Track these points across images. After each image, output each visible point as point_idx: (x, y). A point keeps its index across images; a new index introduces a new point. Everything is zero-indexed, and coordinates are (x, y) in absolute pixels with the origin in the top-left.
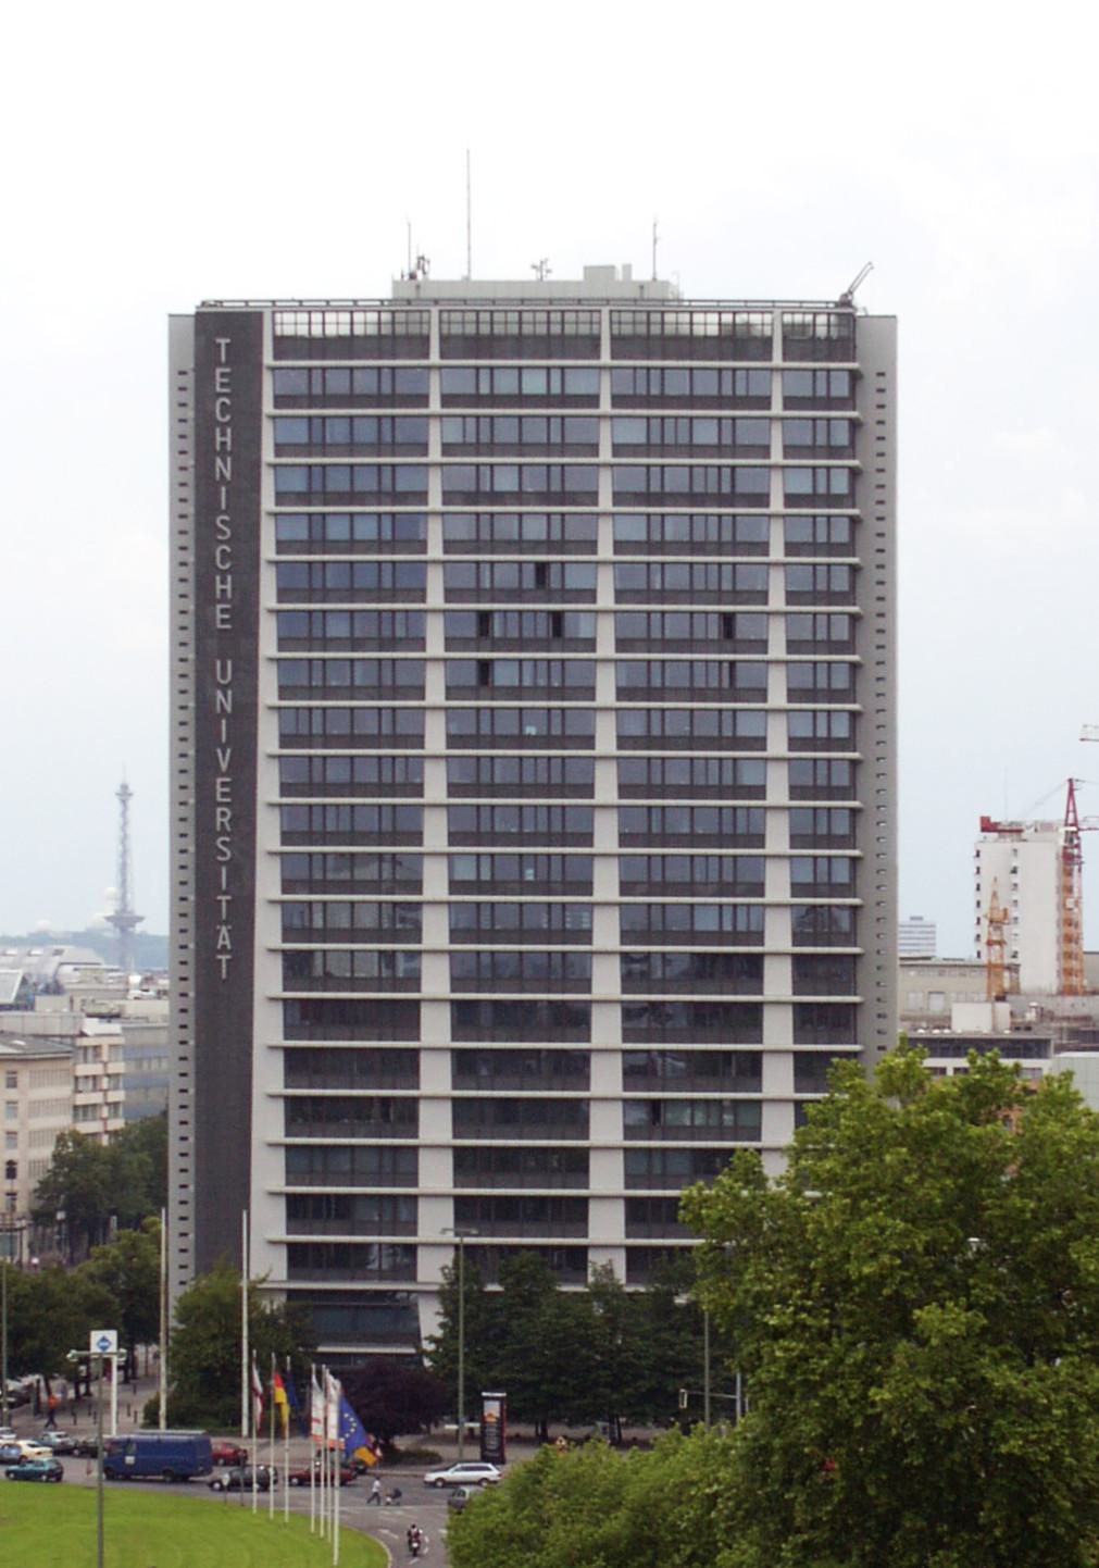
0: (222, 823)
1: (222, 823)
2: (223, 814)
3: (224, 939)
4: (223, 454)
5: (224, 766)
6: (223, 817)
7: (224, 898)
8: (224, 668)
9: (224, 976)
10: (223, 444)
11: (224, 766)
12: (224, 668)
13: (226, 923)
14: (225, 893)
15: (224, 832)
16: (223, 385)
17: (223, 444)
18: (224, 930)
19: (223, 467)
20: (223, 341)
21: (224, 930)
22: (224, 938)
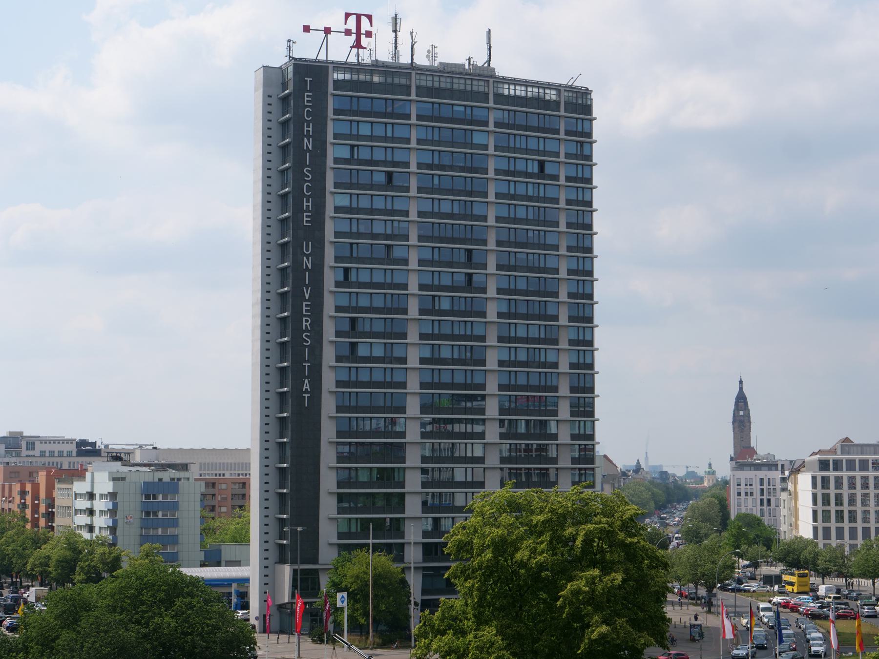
0: (306, 325)
1: (306, 325)
2: (308, 321)
3: (306, 386)
4: (308, 137)
5: (307, 297)
6: (306, 323)
7: (307, 365)
9: (306, 406)
11: (307, 297)
13: (307, 377)
15: (307, 330)
18: (306, 380)
20: (309, 79)
21: (306, 380)
22: (306, 385)
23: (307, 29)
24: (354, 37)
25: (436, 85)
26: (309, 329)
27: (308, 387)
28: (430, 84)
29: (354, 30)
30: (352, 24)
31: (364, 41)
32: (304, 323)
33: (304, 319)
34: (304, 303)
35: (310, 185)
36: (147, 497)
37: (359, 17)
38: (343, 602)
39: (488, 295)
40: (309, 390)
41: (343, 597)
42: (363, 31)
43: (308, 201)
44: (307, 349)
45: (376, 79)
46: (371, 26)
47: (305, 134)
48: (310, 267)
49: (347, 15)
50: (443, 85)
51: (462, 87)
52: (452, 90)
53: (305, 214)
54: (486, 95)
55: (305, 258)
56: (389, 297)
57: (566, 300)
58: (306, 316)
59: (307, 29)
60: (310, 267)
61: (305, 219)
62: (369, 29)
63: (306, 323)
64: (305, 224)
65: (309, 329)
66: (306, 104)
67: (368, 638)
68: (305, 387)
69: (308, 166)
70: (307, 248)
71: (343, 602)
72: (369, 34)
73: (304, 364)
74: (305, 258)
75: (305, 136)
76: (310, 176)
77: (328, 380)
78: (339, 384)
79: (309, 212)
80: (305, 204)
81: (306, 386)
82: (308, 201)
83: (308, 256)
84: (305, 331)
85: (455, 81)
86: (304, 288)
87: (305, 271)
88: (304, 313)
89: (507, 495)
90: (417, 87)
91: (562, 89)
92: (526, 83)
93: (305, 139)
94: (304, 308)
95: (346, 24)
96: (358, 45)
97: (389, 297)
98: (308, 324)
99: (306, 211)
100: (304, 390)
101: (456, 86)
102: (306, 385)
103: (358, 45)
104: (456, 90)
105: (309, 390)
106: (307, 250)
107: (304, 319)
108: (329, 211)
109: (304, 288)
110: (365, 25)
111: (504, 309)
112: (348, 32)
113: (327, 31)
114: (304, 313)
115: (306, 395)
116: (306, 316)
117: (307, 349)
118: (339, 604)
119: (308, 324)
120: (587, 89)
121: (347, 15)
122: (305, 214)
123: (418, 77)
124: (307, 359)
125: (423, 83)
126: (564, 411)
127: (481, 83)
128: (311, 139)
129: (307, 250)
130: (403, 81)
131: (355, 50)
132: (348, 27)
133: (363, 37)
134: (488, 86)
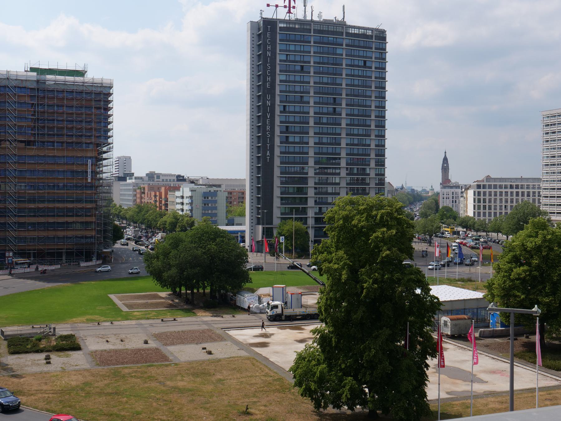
2: (268, 127)
4: (269, 51)
5: (268, 117)
6: (268, 128)
7: (268, 145)
10: (269, 49)
11: (268, 117)
15: (268, 131)
16: (269, 36)
17: (269, 49)
18: (268, 152)
20: (269, 27)
21: (268, 152)
22: (268, 154)
24: (288, 8)
25: (322, 29)
28: (319, 28)
29: (288, 6)
31: (292, 10)
36: (205, 198)
38: (282, 240)
39: (342, 116)
41: (283, 238)
42: (292, 6)
43: (269, 78)
45: (297, 26)
50: (324, 29)
51: (332, 30)
52: (328, 31)
54: (343, 33)
55: (268, 101)
56: (302, 117)
58: (268, 125)
59: (268, 5)
62: (294, 5)
63: (268, 128)
67: (292, 255)
69: (269, 63)
70: (269, 97)
71: (282, 240)
72: (294, 7)
74: (268, 101)
77: (277, 151)
78: (281, 153)
79: (269, 82)
82: (269, 78)
83: (269, 101)
85: (330, 27)
90: (314, 30)
91: (374, 30)
92: (359, 28)
93: (268, 52)
94: (267, 122)
96: (289, 12)
97: (302, 117)
99: (268, 82)
101: (330, 29)
102: (268, 154)
103: (289, 12)
104: (330, 31)
106: (269, 98)
108: (278, 82)
111: (349, 122)
112: (285, 7)
113: (277, 6)
115: (268, 157)
116: (268, 125)
118: (281, 241)
120: (384, 30)
123: (314, 25)
125: (316, 28)
126: (373, 164)
127: (340, 28)
129: (269, 98)
130: (308, 27)
131: (288, 14)
133: (291, 9)
134: (343, 29)
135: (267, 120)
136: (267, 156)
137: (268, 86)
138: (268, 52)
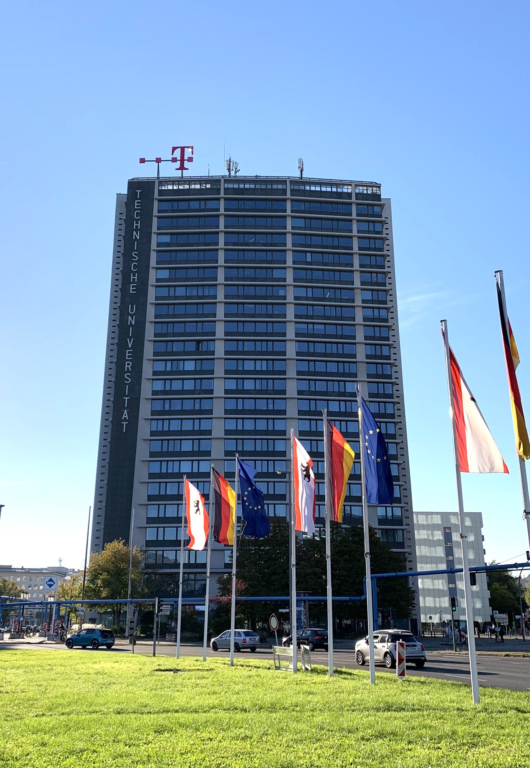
0: (128, 368)
1: (128, 368)
2: (129, 364)
3: (125, 415)
4: (137, 230)
5: (130, 346)
6: (128, 366)
7: (126, 398)
8: (132, 308)
10: (137, 227)
11: (130, 346)
12: (132, 308)
13: (126, 408)
14: (127, 396)
15: (128, 371)
16: (137, 206)
17: (137, 227)
19: (136, 235)
20: (139, 191)
22: (125, 415)
23: (142, 161)
24: (179, 162)
26: (130, 370)
27: (127, 416)
29: (179, 158)
30: (177, 154)
31: (186, 164)
32: (126, 366)
33: (127, 362)
34: (127, 351)
35: (137, 264)
37: (183, 149)
40: (127, 419)
42: (186, 158)
43: (134, 276)
44: (127, 386)
46: (193, 154)
47: (134, 228)
48: (133, 323)
49: (174, 149)
53: (131, 285)
55: (130, 317)
57: (363, 341)
58: (128, 360)
59: (142, 161)
60: (133, 323)
61: (131, 288)
62: (191, 156)
64: (131, 292)
65: (130, 370)
66: (136, 208)
68: (124, 417)
72: (190, 160)
73: (124, 398)
74: (130, 317)
75: (134, 230)
76: (133, 255)
79: (135, 283)
80: (132, 278)
81: (125, 415)
82: (134, 276)
84: (127, 372)
86: (128, 339)
87: (130, 326)
88: (127, 358)
89: (247, 574)
93: (135, 232)
95: (172, 155)
96: (182, 168)
98: (129, 366)
99: (132, 283)
100: (123, 419)
102: (125, 415)
103: (182, 168)
105: (127, 419)
107: (127, 362)
108: (152, 280)
109: (128, 339)
110: (188, 153)
112: (174, 160)
113: (158, 160)
114: (127, 358)
115: (125, 423)
116: (128, 360)
117: (127, 386)
119: (129, 366)
121: (174, 149)
122: (131, 285)
124: (127, 394)
126: (63, 655)
128: (139, 232)
132: (174, 156)
135: (127, 351)
136: (124, 421)
137: (133, 290)
138: (135, 232)
